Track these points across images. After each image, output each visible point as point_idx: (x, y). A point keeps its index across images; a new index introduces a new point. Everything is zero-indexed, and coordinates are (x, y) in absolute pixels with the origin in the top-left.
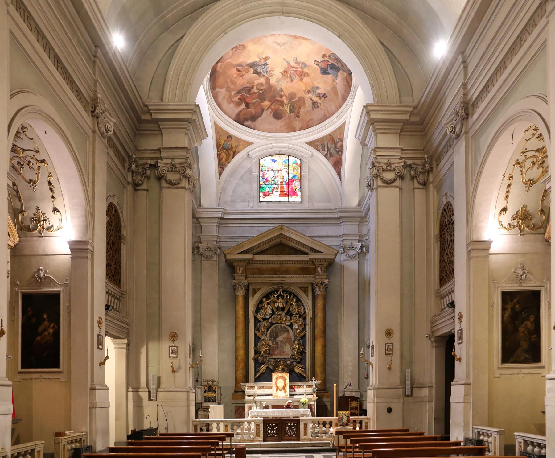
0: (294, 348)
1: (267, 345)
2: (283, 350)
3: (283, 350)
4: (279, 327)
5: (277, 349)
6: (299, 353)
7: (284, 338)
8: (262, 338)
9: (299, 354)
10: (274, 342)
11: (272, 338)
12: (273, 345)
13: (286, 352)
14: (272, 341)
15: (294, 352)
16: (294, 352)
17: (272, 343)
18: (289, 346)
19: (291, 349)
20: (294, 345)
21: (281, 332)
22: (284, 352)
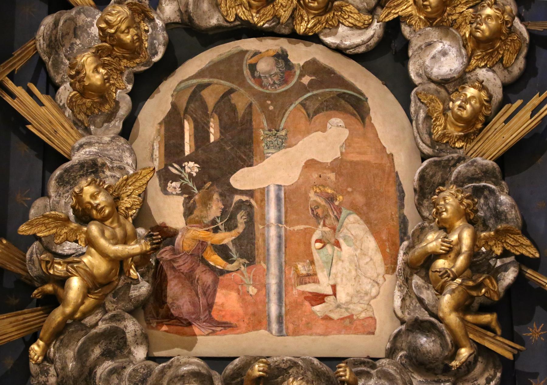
0: (433, 257)
1: (136, 223)
2: (312, 277)
3: (303, 279)
4: (263, 66)
5: (238, 263)
6: (483, 309)
7: (311, 164)
8: (77, 157)
9: (486, 318)
10: (206, 202)
11: (192, 167)
12: (201, 233)
13: (342, 296)
14: (185, 189)
15: (428, 295)
16: (428, 295)
17: (189, 211)
18: (371, 243)
19: (391, 268)
20: (422, 231)
21: (283, 110)
22: (319, 298)
